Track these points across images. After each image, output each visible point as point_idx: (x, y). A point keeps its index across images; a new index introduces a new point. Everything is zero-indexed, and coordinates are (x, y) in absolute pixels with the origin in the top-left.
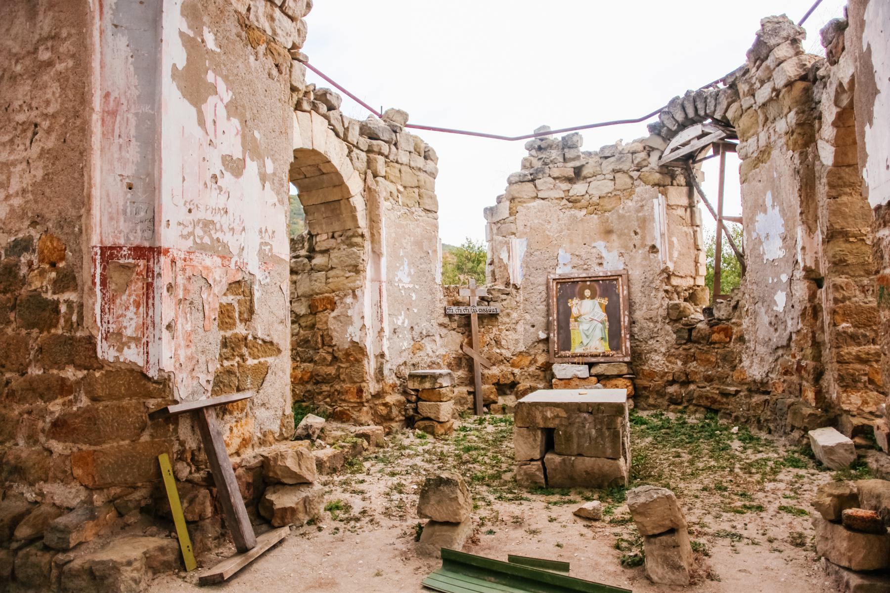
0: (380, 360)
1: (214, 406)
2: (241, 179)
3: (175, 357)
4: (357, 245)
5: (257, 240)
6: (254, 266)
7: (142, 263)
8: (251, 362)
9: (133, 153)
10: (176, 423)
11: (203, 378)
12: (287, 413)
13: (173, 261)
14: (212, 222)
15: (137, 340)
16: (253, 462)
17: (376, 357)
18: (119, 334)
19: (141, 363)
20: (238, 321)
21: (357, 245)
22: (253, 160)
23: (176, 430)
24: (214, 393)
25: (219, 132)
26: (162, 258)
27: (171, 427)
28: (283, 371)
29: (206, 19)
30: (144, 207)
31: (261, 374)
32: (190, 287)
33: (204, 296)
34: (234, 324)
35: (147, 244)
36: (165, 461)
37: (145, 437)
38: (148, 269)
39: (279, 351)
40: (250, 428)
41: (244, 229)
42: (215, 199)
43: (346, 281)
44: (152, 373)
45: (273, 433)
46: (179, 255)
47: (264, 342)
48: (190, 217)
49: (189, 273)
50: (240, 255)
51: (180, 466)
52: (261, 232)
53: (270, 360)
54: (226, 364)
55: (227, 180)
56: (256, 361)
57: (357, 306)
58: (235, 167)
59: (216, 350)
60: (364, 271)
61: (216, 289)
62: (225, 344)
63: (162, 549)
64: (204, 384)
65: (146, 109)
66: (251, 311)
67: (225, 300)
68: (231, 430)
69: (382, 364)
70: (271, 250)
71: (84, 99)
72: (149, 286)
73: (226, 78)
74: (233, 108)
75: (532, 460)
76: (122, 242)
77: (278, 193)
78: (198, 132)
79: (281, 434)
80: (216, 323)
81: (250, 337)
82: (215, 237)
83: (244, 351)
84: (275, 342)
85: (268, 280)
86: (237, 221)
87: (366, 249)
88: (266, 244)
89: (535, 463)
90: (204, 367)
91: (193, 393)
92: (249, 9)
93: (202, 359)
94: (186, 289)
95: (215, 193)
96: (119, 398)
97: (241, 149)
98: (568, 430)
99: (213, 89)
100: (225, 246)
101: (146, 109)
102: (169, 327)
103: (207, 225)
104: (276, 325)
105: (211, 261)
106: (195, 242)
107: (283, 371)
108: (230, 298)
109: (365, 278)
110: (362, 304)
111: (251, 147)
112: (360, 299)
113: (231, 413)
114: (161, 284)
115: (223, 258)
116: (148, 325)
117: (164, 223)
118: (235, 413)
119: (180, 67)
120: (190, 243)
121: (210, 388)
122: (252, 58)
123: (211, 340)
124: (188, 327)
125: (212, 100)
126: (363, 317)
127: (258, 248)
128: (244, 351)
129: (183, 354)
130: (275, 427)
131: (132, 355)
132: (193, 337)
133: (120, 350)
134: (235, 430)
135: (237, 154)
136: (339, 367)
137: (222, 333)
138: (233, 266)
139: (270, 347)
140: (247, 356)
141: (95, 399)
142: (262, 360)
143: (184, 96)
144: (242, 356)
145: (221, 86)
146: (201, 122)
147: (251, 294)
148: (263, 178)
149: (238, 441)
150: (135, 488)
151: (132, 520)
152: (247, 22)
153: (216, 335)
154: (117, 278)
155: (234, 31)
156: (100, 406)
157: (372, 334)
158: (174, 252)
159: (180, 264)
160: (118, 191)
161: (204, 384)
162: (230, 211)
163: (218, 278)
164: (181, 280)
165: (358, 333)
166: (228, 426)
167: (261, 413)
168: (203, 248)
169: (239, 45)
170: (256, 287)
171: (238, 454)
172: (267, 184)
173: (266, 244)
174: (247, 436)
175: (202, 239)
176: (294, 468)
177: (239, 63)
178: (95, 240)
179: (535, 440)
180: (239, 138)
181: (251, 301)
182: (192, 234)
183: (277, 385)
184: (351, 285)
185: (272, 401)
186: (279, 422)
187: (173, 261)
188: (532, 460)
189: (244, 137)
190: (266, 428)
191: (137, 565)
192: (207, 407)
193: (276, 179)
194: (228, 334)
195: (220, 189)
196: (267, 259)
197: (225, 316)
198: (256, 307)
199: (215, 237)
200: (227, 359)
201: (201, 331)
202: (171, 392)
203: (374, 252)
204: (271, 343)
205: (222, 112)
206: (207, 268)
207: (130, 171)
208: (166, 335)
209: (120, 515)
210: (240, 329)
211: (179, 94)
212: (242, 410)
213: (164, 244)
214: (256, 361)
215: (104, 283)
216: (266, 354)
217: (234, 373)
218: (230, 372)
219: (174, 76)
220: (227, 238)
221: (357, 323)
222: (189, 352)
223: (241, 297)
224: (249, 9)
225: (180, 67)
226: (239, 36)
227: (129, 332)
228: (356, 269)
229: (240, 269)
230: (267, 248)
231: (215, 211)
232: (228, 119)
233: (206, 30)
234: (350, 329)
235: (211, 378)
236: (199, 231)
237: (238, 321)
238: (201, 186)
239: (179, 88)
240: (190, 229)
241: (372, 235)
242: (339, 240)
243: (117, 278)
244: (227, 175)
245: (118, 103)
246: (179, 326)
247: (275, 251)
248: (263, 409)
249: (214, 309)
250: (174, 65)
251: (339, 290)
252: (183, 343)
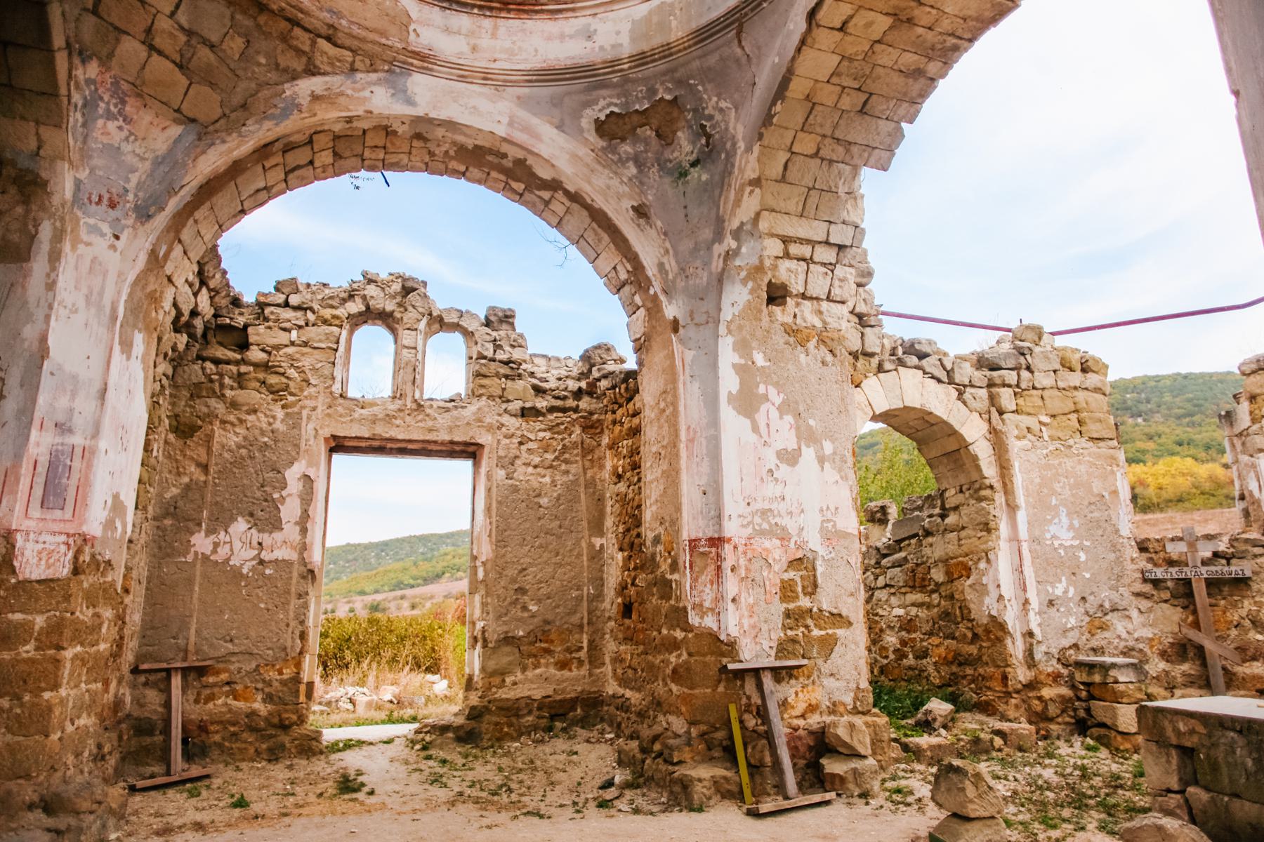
0: (1029, 639)
1: (772, 669)
2: (797, 468)
3: (740, 624)
4: (985, 499)
5: (819, 518)
6: (815, 542)
7: (713, 550)
8: (816, 632)
9: (705, 467)
10: (743, 680)
11: (766, 645)
12: (862, 686)
13: (735, 547)
14: (770, 510)
15: (712, 610)
16: (815, 727)
17: (1024, 635)
18: (701, 605)
19: (715, 629)
20: (801, 595)
21: (985, 499)
22: (808, 446)
23: (742, 686)
24: (777, 658)
25: (773, 430)
26: (726, 546)
27: (739, 683)
28: (856, 644)
29: (754, 344)
30: (713, 506)
31: (828, 645)
32: (752, 567)
33: (765, 574)
34: (797, 597)
35: (716, 536)
36: (732, 708)
37: (721, 689)
38: (718, 555)
39: (850, 624)
40: (817, 695)
41: (802, 511)
42: (771, 490)
43: (978, 543)
44: (723, 637)
45: (844, 705)
46: (740, 542)
47: (832, 614)
48: (749, 509)
49: (750, 555)
50: (799, 535)
51: (746, 716)
52: (821, 510)
53: (840, 632)
54: (789, 633)
55: (784, 471)
56: (823, 633)
57: (991, 572)
58: (790, 458)
59: (779, 620)
60: (997, 529)
61: (776, 568)
62: (788, 614)
63: (725, 778)
64: (767, 649)
65: (712, 432)
66: (815, 586)
67: (786, 576)
68: (797, 693)
69: (1031, 645)
70: (834, 526)
71: (676, 434)
72: (719, 568)
73: (776, 385)
74: (782, 410)
75: (1169, 791)
76: (700, 535)
77: (840, 471)
78: (753, 438)
79: (855, 707)
80: (778, 597)
81: (815, 610)
82: (773, 522)
83: (809, 622)
84: (844, 614)
85: (833, 555)
86: (795, 505)
87: (998, 502)
88: (828, 521)
89: (1173, 795)
90: (767, 635)
91: (757, 656)
92: (795, 316)
93: (765, 627)
94: (747, 569)
95: (771, 485)
96: (704, 655)
97: (795, 440)
98: (1212, 752)
99: (766, 398)
100: (784, 529)
101: (712, 432)
102: (734, 600)
103: (764, 513)
104: (844, 597)
105: (771, 544)
106: (754, 529)
107: (856, 644)
108: (791, 574)
109: (998, 537)
110: (997, 570)
111: (807, 436)
112: (993, 563)
113: (797, 678)
114: (727, 566)
115: (782, 539)
116: (719, 598)
117: (726, 518)
118: (801, 679)
119: (734, 392)
120: (749, 530)
121: (773, 653)
122: (802, 356)
123: (773, 611)
124: (751, 600)
125: (763, 408)
126: (999, 586)
127: (819, 526)
128: (809, 622)
129: (746, 622)
130: (848, 699)
131: (710, 622)
132: (755, 609)
133: (702, 618)
134: (800, 694)
135: (792, 445)
136: (981, 647)
137: (785, 605)
138: (792, 545)
139: (838, 619)
140: (812, 627)
141: (690, 654)
142: (830, 631)
143: (739, 413)
144: (807, 627)
145: (772, 392)
146: (755, 429)
147: (814, 569)
148: (821, 460)
149: (804, 705)
150: (717, 729)
151: (716, 755)
152: (795, 328)
153: (779, 608)
154: (699, 562)
155: (782, 341)
156: (692, 660)
157: (1015, 607)
158: (736, 540)
159: (741, 548)
160: (697, 495)
161: (767, 649)
162: (787, 498)
163: (777, 558)
164: (742, 562)
165: (995, 605)
166: (793, 690)
167: (830, 683)
168: (762, 533)
169: (788, 350)
170: (819, 563)
171: (803, 716)
172: (827, 465)
173: (828, 521)
174: (814, 702)
175: (760, 525)
176: (847, 738)
177: (790, 366)
178: (685, 536)
179: (1168, 762)
180: (793, 431)
181: (815, 576)
182: (751, 522)
183: (848, 657)
184: (983, 547)
185: (842, 673)
186: (852, 694)
187: (735, 547)
188: (1169, 791)
189: (798, 429)
190: (836, 698)
191: (706, 783)
192: (764, 669)
193: (837, 458)
194: (791, 606)
195: (777, 480)
196: (831, 535)
197: (787, 592)
198: (820, 581)
199: (773, 522)
200: (791, 629)
201: (762, 603)
202: (737, 653)
203: (1008, 505)
204: (840, 615)
205: (774, 413)
206: (766, 550)
207: (704, 481)
208: (731, 606)
209: (710, 749)
210: (804, 602)
211: (735, 413)
212: (809, 677)
213: (727, 534)
214: (823, 633)
215: (691, 567)
216: (834, 625)
217: (799, 642)
218: (794, 641)
219: (729, 402)
220: (785, 521)
221: (994, 594)
222: (752, 621)
223: (804, 573)
224: (795, 316)
225: (734, 392)
226: (787, 343)
227: (707, 604)
228: (987, 527)
229: (799, 547)
230: (830, 525)
231: (772, 500)
232: (781, 418)
233: (755, 352)
234: (987, 601)
235: (774, 645)
236: (757, 520)
237: (801, 595)
238: (758, 482)
239: (734, 408)
240: (749, 519)
241: (1005, 485)
242: (967, 494)
243: (699, 562)
244: (784, 467)
245: (695, 432)
246: (743, 600)
247: (840, 526)
248: (832, 679)
249: (775, 585)
250: (730, 392)
251: (972, 553)
252: (746, 613)
